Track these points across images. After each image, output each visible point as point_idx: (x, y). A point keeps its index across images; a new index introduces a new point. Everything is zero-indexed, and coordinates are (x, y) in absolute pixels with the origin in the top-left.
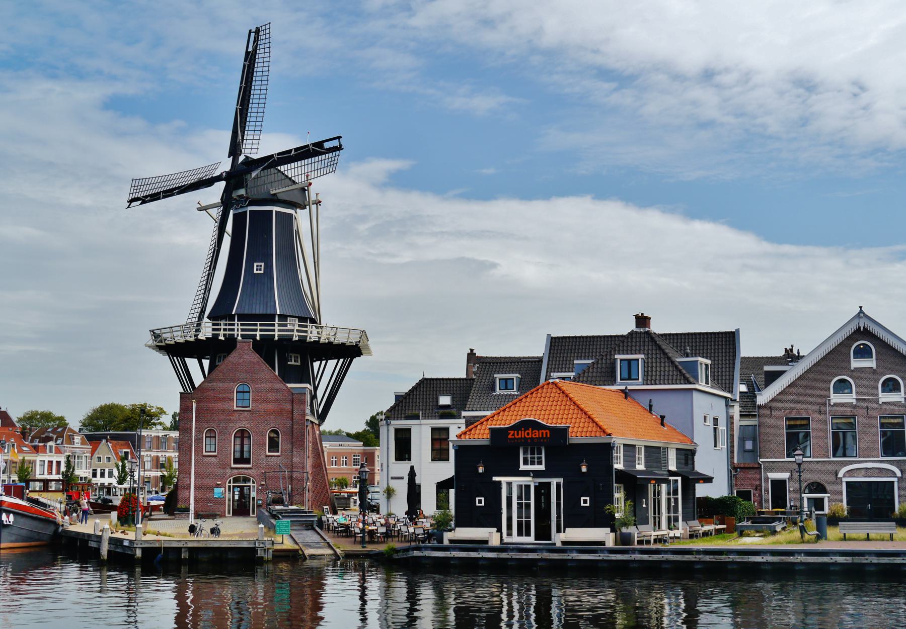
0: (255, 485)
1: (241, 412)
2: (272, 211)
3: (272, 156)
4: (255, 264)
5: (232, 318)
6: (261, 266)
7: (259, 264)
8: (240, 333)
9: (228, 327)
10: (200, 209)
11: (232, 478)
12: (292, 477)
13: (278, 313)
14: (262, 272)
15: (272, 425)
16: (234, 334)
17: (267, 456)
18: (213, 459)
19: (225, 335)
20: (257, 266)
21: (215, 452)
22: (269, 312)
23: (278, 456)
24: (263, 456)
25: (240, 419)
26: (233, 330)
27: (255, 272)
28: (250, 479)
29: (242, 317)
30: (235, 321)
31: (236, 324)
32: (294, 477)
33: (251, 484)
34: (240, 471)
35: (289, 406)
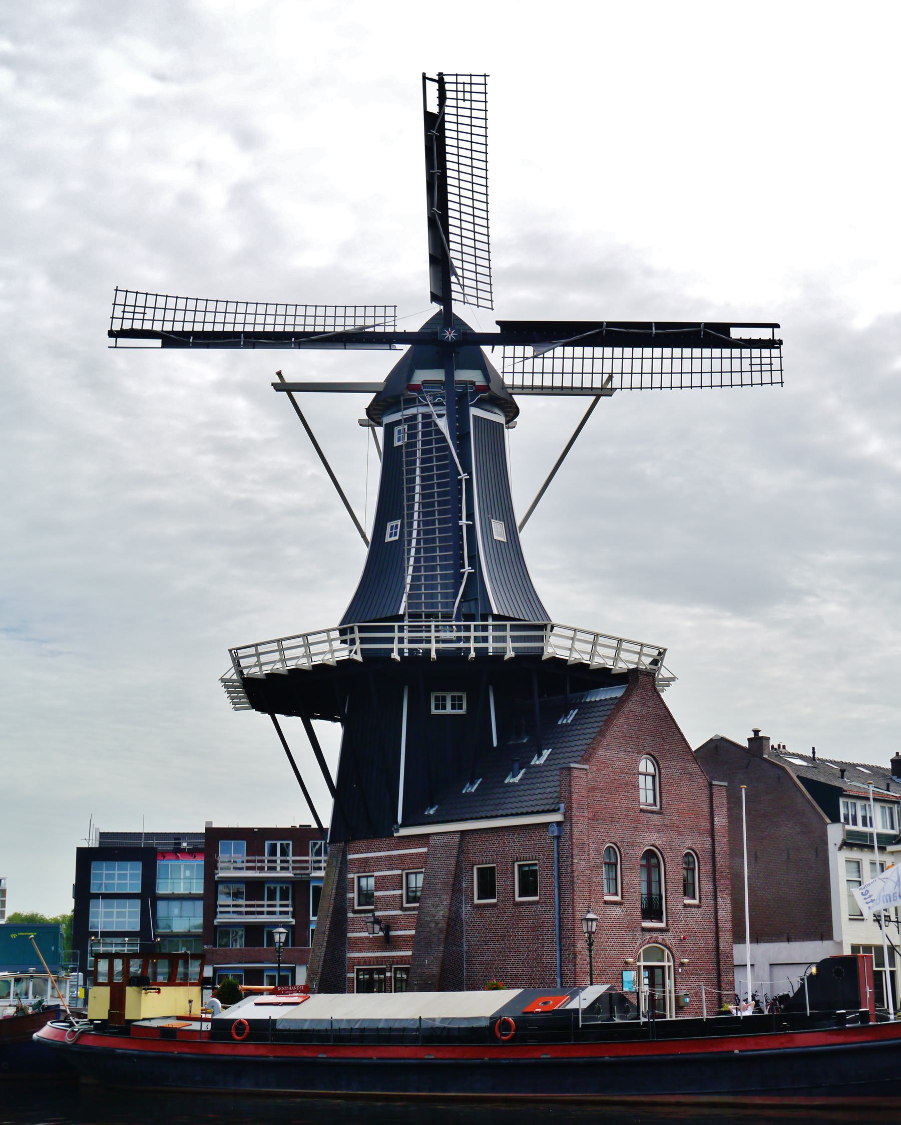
0: (671, 964)
1: (650, 815)
3: (602, 323)
9: (424, 634)
10: (278, 387)
11: (641, 950)
12: (717, 948)
15: (689, 844)
17: (685, 906)
18: (618, 910)
19: (401, 651)
21: (616, 894)
23: (698, 907)
24: (681, 907)
25: (648, 828)
28: (663, 951)
32: (721, 947)
33: (666, 964)
34: (654, 935)
35: (705, 808)
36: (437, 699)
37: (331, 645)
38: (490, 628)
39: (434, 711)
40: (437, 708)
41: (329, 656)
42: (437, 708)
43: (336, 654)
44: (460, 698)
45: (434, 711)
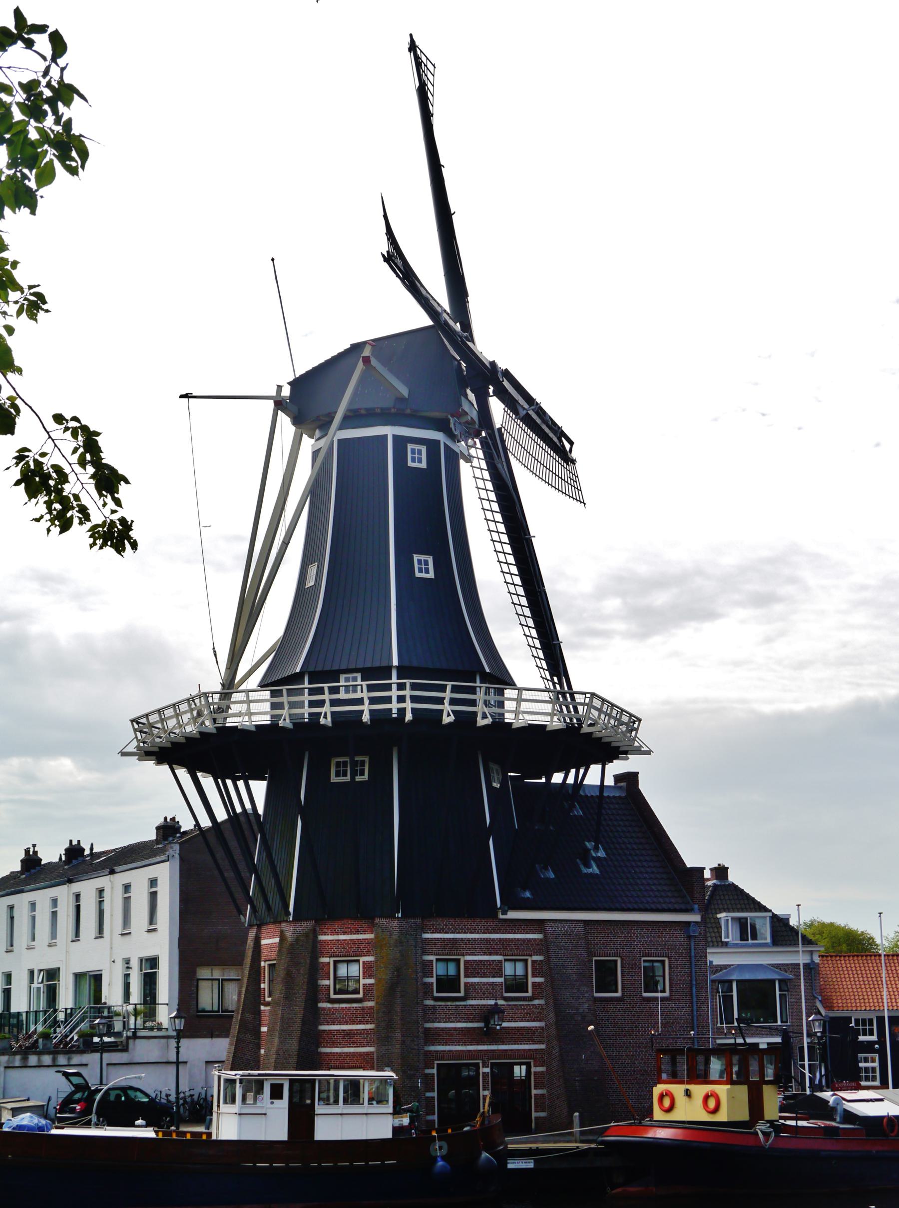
2: (439, 441)
4: (416, 557)
5: (385, 672)
6: (426, 563)
7: (423, 557)
8: (408, 705)
13: (488, 670)
14: (431, 575)
16: (391, 709)
20: (419, 562)
22: (383, 664)
26: (388, 700)
27: (418, 575)
29: (403, 672)
30: (391, 679)
31: (359, 688)
36: (338, 765)
37: (249, 707)
38: (306, 691)
39: (334, 779)
40: (338, 775)
41: (246, 719)
42: (338, 775)
43: (254, 718)
44: (363, 763)
45: (334, 779)
